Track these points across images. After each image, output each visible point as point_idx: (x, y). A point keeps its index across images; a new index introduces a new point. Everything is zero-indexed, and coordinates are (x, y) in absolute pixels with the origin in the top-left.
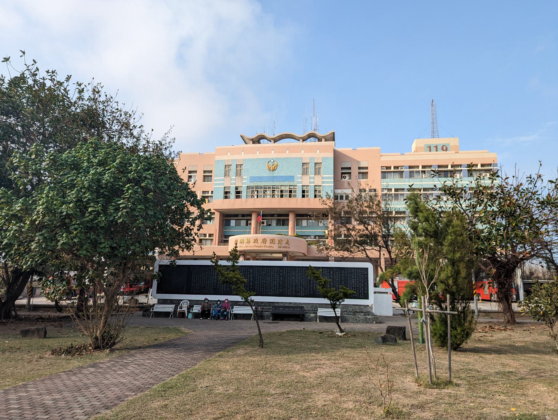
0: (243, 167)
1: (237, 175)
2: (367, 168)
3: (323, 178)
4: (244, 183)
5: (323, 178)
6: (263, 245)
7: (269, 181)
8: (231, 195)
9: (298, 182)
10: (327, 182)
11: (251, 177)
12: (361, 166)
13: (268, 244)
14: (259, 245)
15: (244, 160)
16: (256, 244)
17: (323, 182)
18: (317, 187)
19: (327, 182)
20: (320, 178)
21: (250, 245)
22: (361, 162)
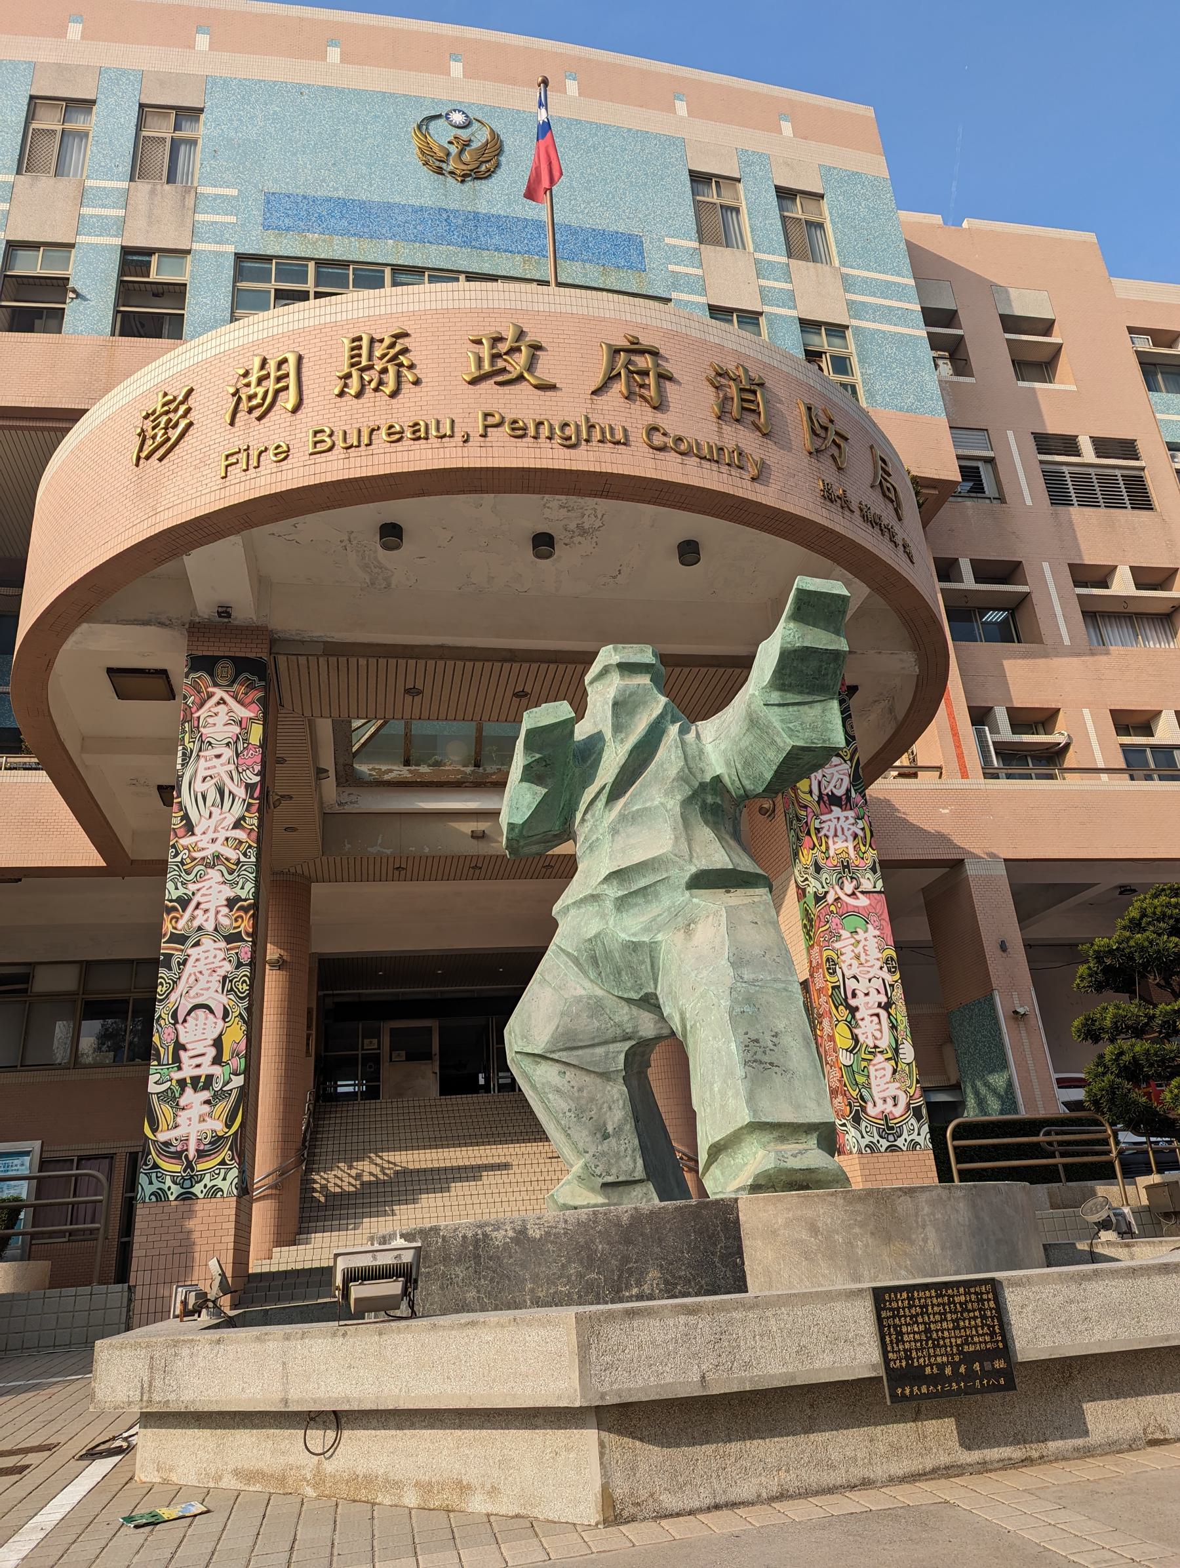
0: (203, 130)
1: (137, 172)
2: (1046, 327)
3: (848, 283)
4: (209, 227)
5: (848, 283)
6: (615, 410)
7: (439, 240)
8: (71, 308)
9: (677, 281)
10: (887, 314)
11: (271, 200)
12: (1018, 311)
13: (692, 412)
14: (570, 406)
15: (209, 83)
16: (521, 403)
17: (853, 308)
18: (821, 341)
19: (887, 314)
20: (834, 287)
21: (409, 408)
22: (1013, 293)
